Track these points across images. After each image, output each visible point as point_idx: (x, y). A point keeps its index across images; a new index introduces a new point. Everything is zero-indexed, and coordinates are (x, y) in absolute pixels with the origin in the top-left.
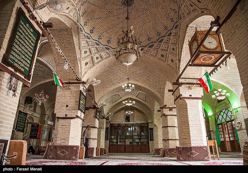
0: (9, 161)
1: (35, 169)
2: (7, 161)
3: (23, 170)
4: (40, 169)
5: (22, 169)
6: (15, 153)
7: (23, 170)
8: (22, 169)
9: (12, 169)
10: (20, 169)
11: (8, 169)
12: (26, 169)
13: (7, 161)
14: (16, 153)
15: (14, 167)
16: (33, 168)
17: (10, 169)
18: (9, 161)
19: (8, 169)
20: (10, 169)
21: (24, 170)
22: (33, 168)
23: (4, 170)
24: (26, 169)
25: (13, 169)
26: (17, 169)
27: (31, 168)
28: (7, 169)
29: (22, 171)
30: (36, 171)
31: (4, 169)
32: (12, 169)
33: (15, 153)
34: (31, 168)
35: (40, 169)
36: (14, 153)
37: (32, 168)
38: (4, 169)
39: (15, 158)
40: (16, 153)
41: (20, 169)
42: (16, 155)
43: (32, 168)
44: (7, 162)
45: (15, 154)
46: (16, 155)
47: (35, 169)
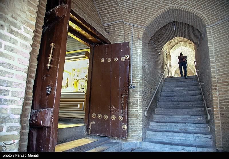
0: (8, 148)
1: (32, 156)
2: (7, 148)
3: (21, 156)
5: (21, 156)
6: (14, 141)
7: (21, 156)
8: (21, 156)
9: (11, 156)
10: (19, 156)
11: (8, 156)
12: (24, 156)
13: (7, 148)
14: (15, 141)
16: (30, 154)
17: (9, 156)
18: (8, 148)
19: (8, 156)
20: (9, 156)
21: (22, 156)
22: (30, 154)
23: (3, 156)
24: (24, 156)
25: (12, 156)
26: (16, 155)
27: (28, 154)
28: (7, 156)
29: (20, 158)
30: (34, 157)
31: (4, 156)
32: (11, 156)
34: (28, 154)
37: (29, 155)
38: (4, 156)
41: (19, 156)
43: (29, 155)
44: (6, 149)
47: (32, 156)
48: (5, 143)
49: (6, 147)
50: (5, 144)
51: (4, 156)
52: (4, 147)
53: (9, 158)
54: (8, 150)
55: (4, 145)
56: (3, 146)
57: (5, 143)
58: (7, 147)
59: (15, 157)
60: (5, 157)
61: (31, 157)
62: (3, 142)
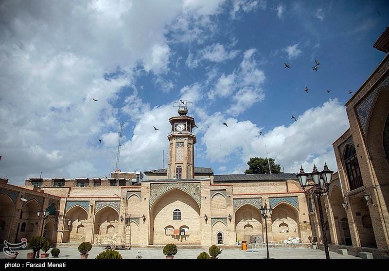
1: (54, 265)
3: (36, 266)
4: (63, 265)
5: (35, 265)
6: (23, 240)
7: (36, 266)
8: (35, 265)
9: (18, 265)
10: (32, 265)
11: (13, 265)
12: (40, 265)
13: (12, 253)
14: (25, 240)
16: (51, 263)
17: (16, 265)
19: (13, 265)
20: (16, 265)
21: (38, 266)
22: (51, 263)
23: (6, 267)
24: (40, 265)
25: (21, 265)
26: (27, 265)
27: (48, 263)
28: (11, 265)
29: (34, 268)
30: (57, 268)
31: (6, 265)
32: (18, 265)
33: (23, 240)
34: (48, 263)
35: (63, 265)
36: (21, 241)
37: (50, 263)
38: (7, 265)
39: (23, 248)
40: (25, 240)
41: (32, 265)
42: (25, 243)
43: (50, 263)
45: (24, 242)
46: (25, 243)
47: (54, 265)
48: (7, 244)
49: (9, 250)
50: (9, 246)
51: (7, 265)
53: (15, 268)
55: (8, 247)
57: (7, 244)
59: (25, 268)
60: (9, 268)
61: (52, 268)
62: (6, 242)
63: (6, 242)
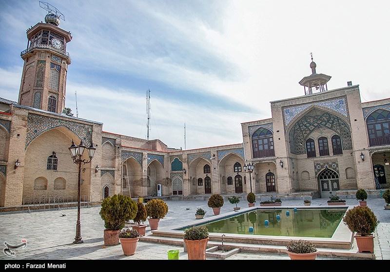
0: (14, 254)
2: (12, 254)
9: (18, 266)
11: (13, 266)
13: (12, 254)
15: (22, 262)
17: (16, 266)
18: (14, 254)
19: (13, 266)
20: (16, 266)
23: (6, 268)
25: (21, 266)
26: (27, 266)
28: (12, 266)
31: (6, 266)
32: (18, 266)
33: (23, 241)
38: (7, 266)
42: (25, 244)
46: (25, 244)
48: (8, 245)
49: (10, 252)
52: (6, 252)
54: (14, 257)
56: (6, 250)
57: (8, 245)
58: (11, 251)
62: (6, 243)
63: (6, 243)
